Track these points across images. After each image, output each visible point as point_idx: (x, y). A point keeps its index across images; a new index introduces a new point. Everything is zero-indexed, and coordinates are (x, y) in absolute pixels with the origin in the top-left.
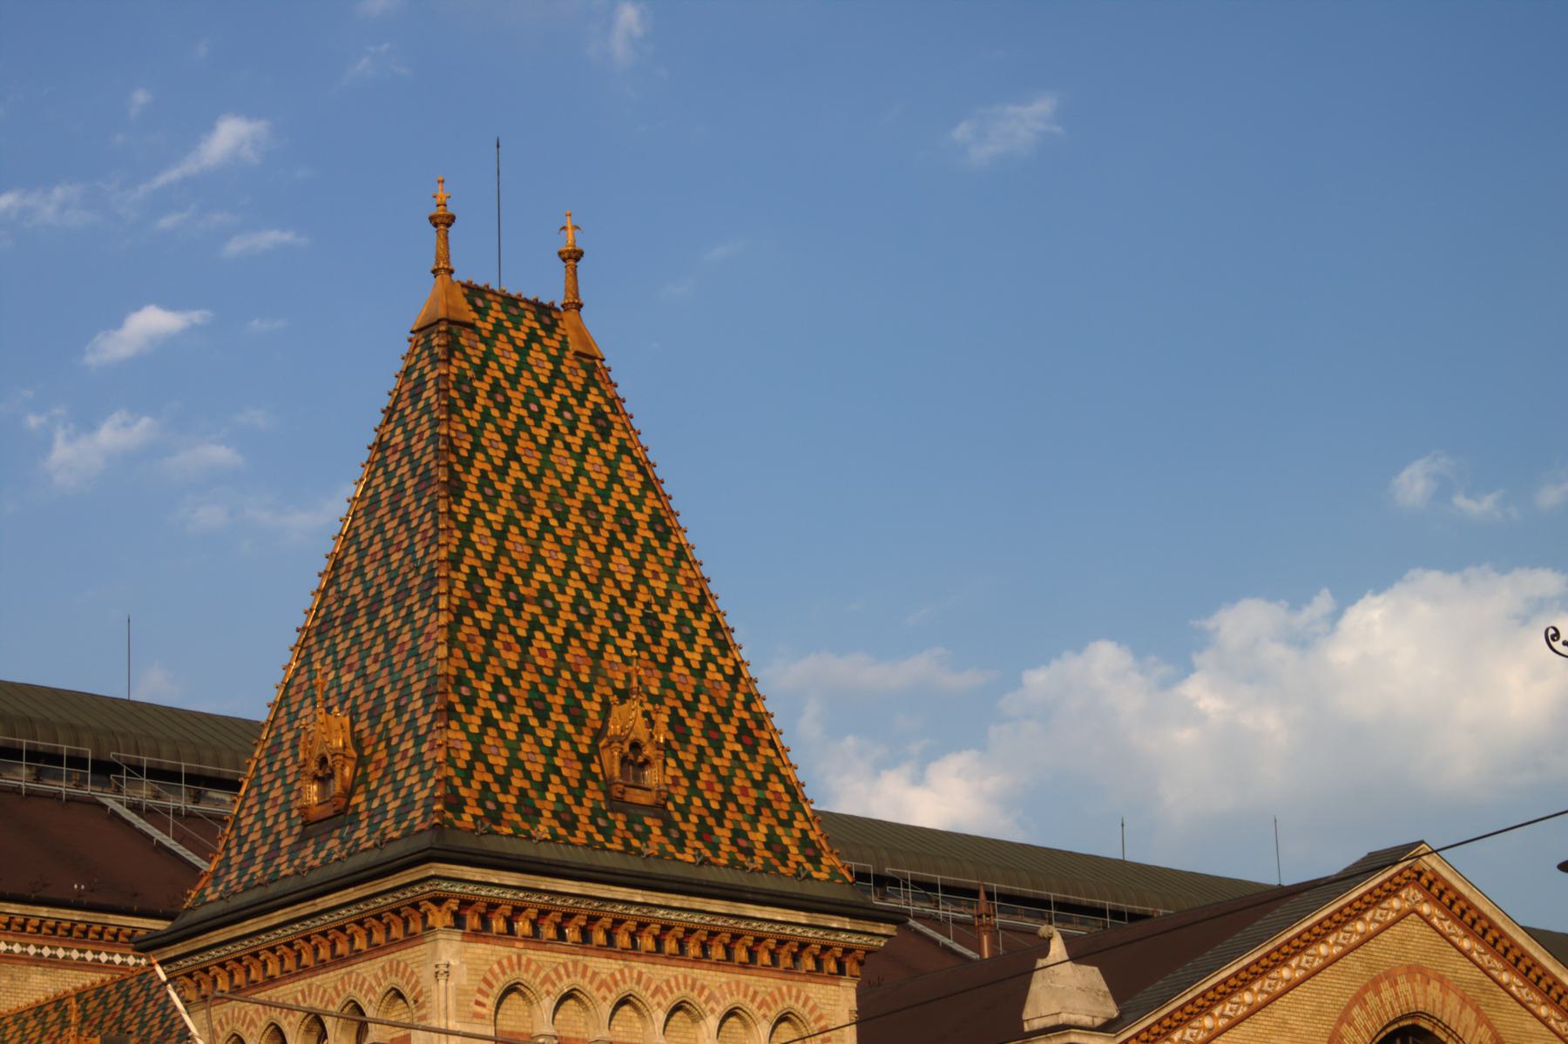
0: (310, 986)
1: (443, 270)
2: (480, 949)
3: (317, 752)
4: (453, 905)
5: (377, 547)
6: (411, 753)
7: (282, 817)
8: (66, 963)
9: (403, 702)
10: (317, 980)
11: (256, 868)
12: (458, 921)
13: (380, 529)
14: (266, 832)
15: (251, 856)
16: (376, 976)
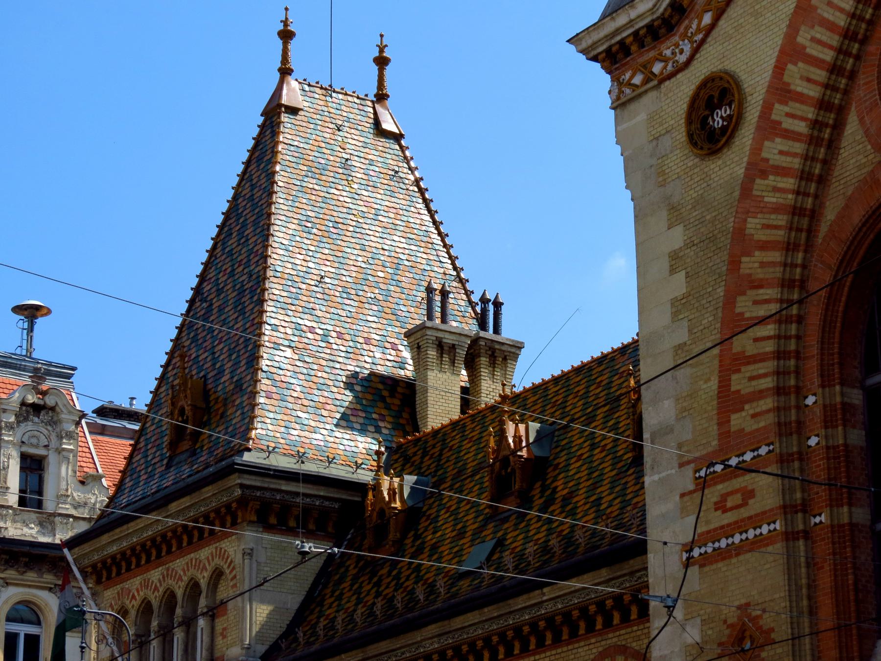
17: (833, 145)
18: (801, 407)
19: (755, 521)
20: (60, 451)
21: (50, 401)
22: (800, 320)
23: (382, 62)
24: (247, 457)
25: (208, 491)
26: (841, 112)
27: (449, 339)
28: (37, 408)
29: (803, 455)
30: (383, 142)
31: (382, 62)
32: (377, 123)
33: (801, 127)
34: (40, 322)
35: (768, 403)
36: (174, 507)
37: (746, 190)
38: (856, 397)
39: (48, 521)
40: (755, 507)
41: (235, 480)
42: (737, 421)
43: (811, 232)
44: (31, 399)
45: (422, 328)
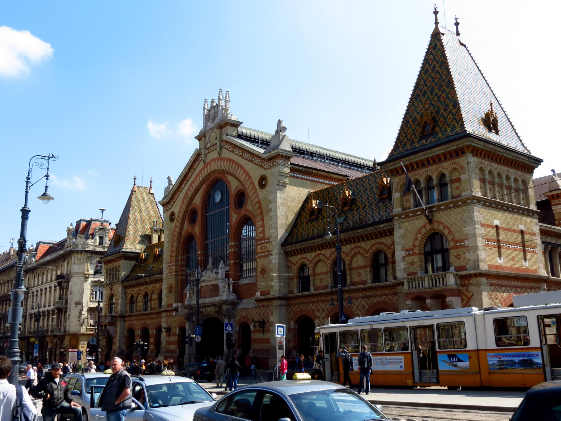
0: (427, 170)
1: (437, 23)
2: (475, 158)
3: (424, 121)
4: (471, 148)
5: (430, 79)
6: (452, 118)
7: (413, 136)
8: (323, 183)
9: (446, 108)
10: (429, 168)
11: (408, 147)
12: (472, 152)
13: (430, 75)
14: (408, 140)
15: (405, 144)
16: (448, 166)
17: (183, 225)
18: (178, 258)
19: (173, 272)
20: (106, 236)
21: (104, 227)
22: (179, 247)
23: (151, 181)
24: (123, 250)
25: (117, 254)
26: (184, 220)
27: (156, 229)
28: (102, 229)
29: (178, 265)
30: (151, 195)
31: (151, 181)
32: (149, 192)
33: (180, 222)
34: (104, 211)
35: (175, 258)
36: (113, 255)
37: (175, 229)
38: (185, 257)
39: (103, 247)
40: (173, 271)
41: (121, 253)
42: (172, 259)
43: (181, 235)
44: (101, 227)
45: (152, 228)
